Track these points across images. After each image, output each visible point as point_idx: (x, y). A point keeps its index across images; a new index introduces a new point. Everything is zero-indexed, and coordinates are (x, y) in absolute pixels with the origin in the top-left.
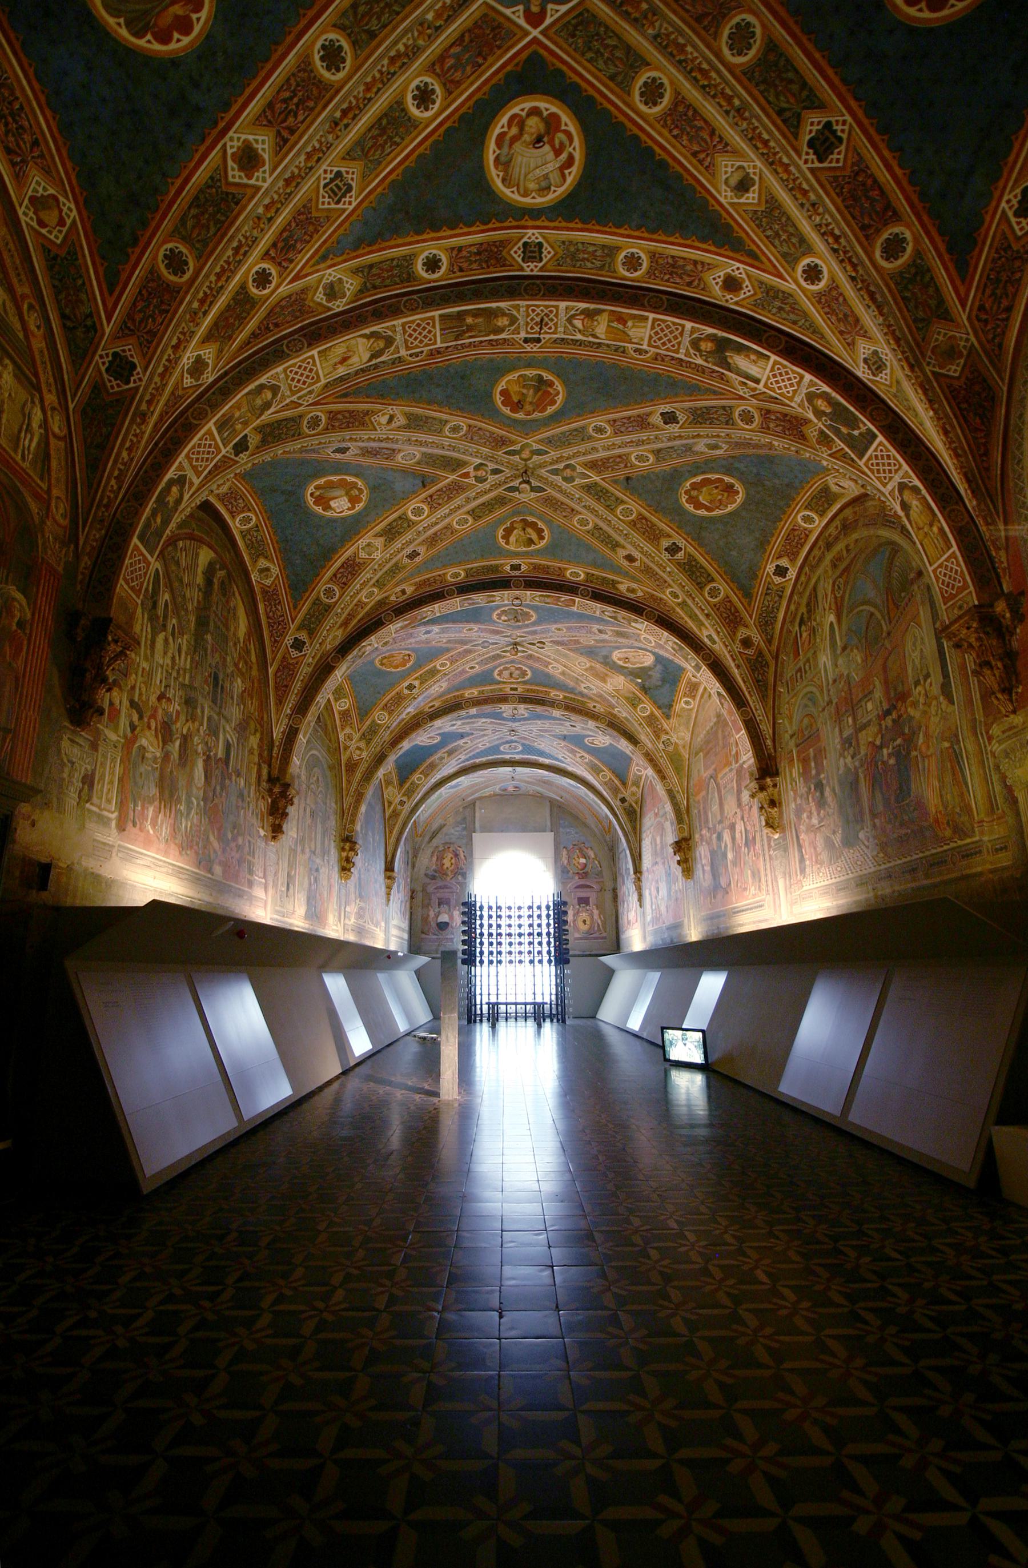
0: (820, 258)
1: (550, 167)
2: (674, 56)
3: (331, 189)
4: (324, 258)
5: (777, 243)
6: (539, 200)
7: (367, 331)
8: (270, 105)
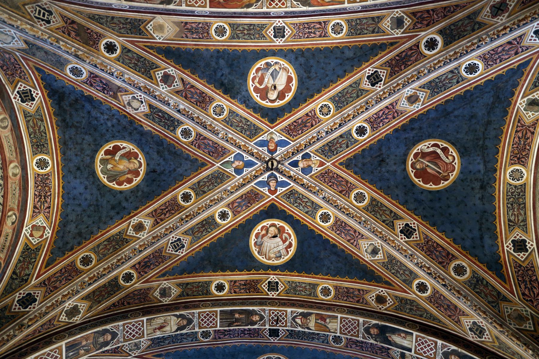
0: (423, 279)
1: (281, 247)
3: (174, 245)
4: (164, 275)
5: (399, 275)
6: (276, 262)
7: (178, 313)
8: (155, 211)
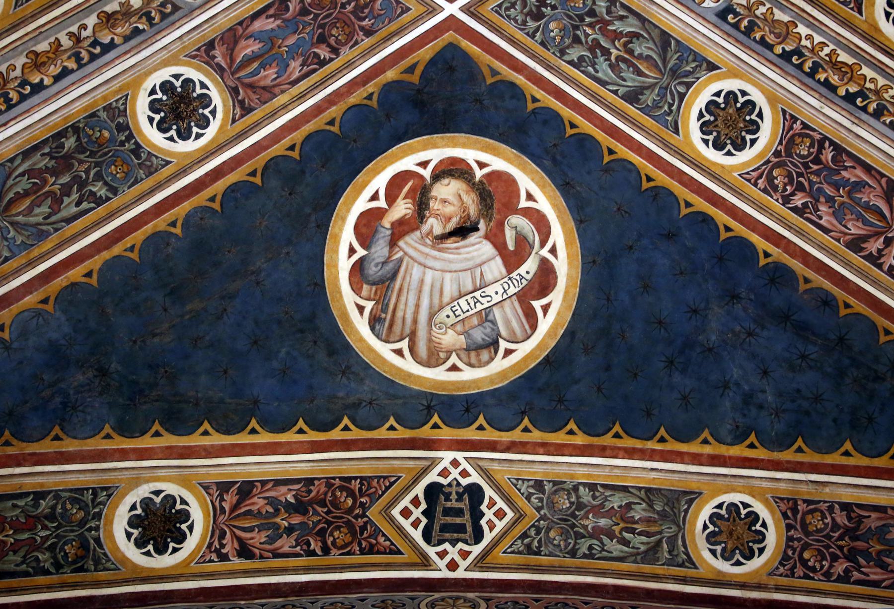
1: (495, 292)
2: (770, 47)
6: (468, 374)
